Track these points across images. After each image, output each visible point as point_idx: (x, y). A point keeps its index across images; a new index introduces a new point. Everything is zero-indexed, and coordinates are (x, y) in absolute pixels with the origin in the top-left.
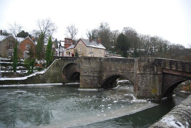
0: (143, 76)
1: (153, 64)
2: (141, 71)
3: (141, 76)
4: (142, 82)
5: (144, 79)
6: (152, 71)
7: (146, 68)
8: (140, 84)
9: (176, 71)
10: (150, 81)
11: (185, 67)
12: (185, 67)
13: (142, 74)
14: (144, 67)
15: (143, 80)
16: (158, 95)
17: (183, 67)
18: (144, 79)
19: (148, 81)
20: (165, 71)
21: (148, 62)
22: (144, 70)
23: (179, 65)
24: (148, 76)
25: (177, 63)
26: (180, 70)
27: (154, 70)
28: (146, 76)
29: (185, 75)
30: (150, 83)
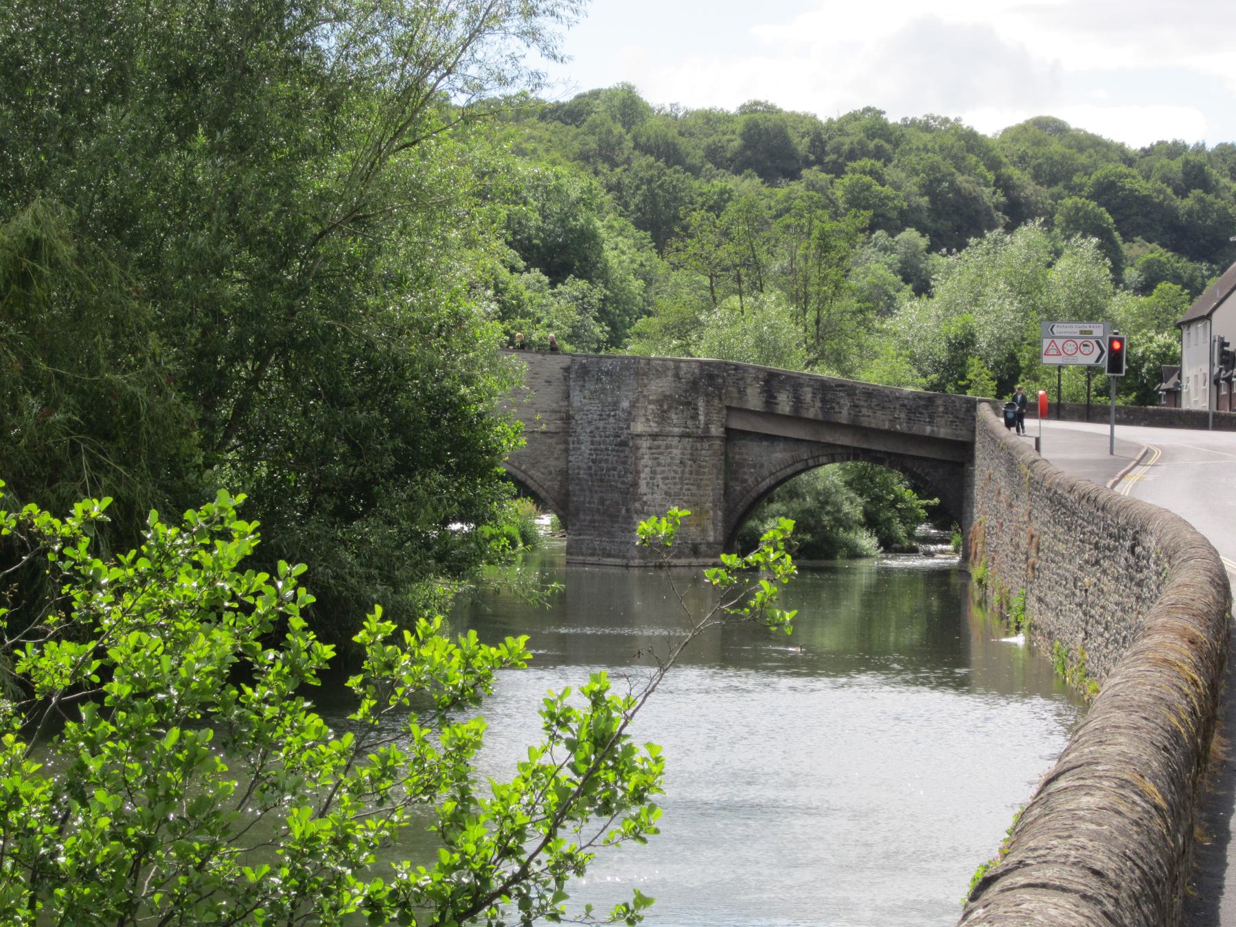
0: (658, 447)
1: (694, 385)
2: (648, 420)
3: (650, 448)
4: (654, 472)
5: (662, 459)
6: (690, 423)
7: (670, 408)
8: (648, 483)
9: (796, 418)
10: (683, 472)
11: (832, 401)
12: (832, 401)
13: (654, 436)
14: (659, 402)
15: (659, 465)
16: (711, 539)
17: (823, 401)
18: (662, 459)
19: (676, 472)
20: (737, 424)
21: (677, 376)
22: (662, 417)
23: (807, 394)
24: (676, 447)
25: (800, 385)
26: (811, 414)
27: (695, 417)
28: (667, 447)
29: (828, 438)
30: (681, 478)
